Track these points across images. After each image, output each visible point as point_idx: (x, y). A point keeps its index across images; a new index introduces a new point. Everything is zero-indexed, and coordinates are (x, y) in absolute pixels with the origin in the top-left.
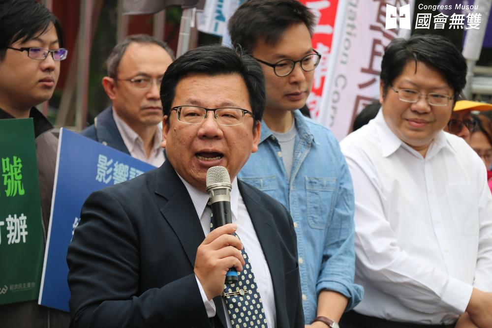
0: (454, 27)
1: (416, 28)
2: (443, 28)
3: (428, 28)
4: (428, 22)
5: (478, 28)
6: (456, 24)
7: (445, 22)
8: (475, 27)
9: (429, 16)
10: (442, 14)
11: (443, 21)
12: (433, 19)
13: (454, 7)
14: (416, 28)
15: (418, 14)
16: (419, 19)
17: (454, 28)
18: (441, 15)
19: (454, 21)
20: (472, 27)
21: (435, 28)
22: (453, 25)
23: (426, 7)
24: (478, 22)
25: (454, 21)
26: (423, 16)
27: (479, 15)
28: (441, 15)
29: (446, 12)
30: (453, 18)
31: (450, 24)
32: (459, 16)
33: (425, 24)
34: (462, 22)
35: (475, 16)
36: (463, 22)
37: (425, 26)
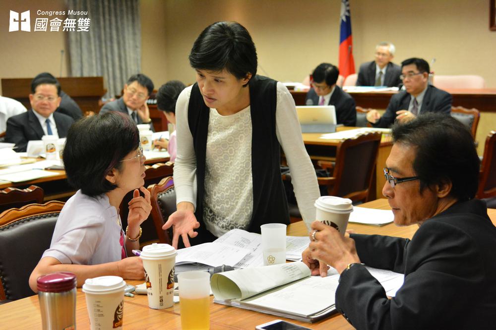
1: (35, 30)
3: (45, 30)
4: (45, 26)
5: (88, 31)
6: (68, 27)
7: (60, 25)
8: (85, 30)
9: (46, 20)
11: (57, 25)
12: (49, 23)
13: (67, 13)
15: (37, 19)
17: (67, 30)
18: (56, 20)
19: (67, 25)
20: (82, 30)
21: (51, 30)
22: (66, 28)
23: (43, 13)
24: (87, 25)
25: (67, 25)
26: (41, 20)
27: (88, 19)
28: (56, 20)
29: (59, 17)
32: (72, 20)
33: (42, 27)
36: (75, 25)
37: (42, 29)
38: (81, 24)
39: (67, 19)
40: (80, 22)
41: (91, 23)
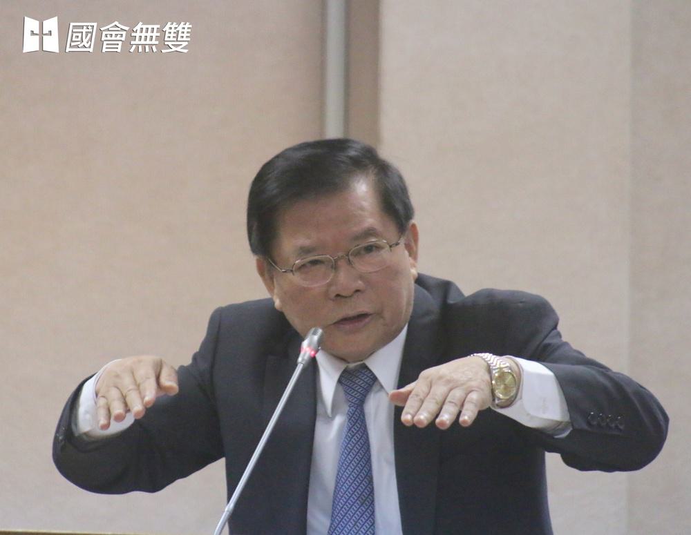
0: (140, 47)
1: (68, 49)
2: (119, 50)
3: (91, 50)
5: (185, 51)
6: (143, 42)
7: (123, 39)
8: (178, 49)
10: (116, 23)
11: (118, 38)
12: (100, 32)
14: (67, 51)
16: (72, 32)
20: (174, 49)
24: (185, 39)
27: (188, 25)
30: (139, 31)
31: (132, 43)
32: (150, 27)
34: (154, 38)
35: (180, 28)
38: (172, 35)
39: (140, 25)
40: (168, 31)
41: (193, 34)
